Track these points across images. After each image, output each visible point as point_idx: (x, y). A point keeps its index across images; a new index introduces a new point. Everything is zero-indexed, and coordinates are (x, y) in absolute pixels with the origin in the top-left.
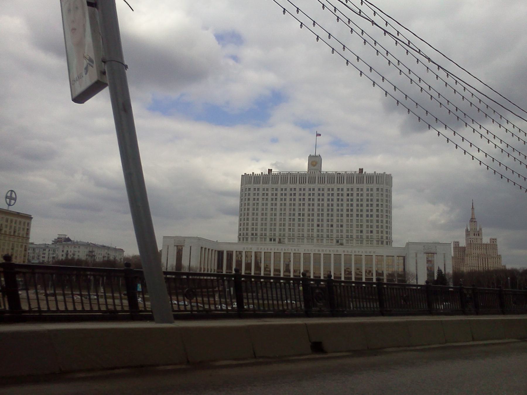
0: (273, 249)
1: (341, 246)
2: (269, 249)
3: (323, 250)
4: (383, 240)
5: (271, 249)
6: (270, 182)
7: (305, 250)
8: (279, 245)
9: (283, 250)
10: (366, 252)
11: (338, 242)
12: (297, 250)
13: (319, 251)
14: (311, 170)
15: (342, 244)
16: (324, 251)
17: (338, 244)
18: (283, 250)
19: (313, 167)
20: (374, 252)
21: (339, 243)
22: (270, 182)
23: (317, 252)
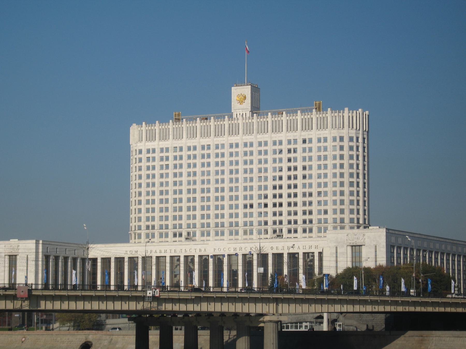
0: (168, 251)
1: (278, 240)
2: (163, 251)
3: (240, 249)
4: (345, 224)
5: (166, 251)
6: (171, 137)
7: (215, 249)
8: (187, 243)
9: (183, 251)
10: (304, 248)
11: (275, 232)
12: (203, 250)
13: (235, 249)
14: (237, 111)
15: (280, 236)
16: (243, 249)
17: (275, 235)
18: (183, 251)
19: (238, 106)
20: (316, 247)
21: (278, 234)
22: (171, 137)
23: (232, 252)
